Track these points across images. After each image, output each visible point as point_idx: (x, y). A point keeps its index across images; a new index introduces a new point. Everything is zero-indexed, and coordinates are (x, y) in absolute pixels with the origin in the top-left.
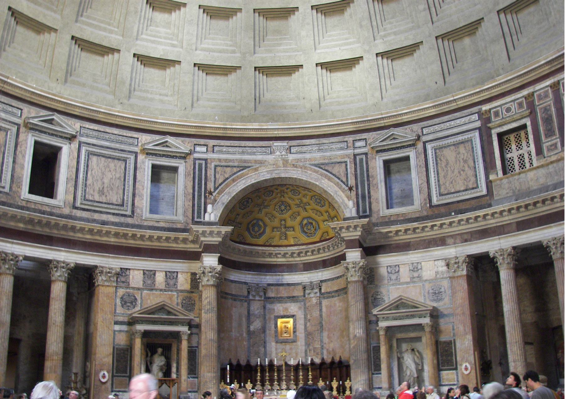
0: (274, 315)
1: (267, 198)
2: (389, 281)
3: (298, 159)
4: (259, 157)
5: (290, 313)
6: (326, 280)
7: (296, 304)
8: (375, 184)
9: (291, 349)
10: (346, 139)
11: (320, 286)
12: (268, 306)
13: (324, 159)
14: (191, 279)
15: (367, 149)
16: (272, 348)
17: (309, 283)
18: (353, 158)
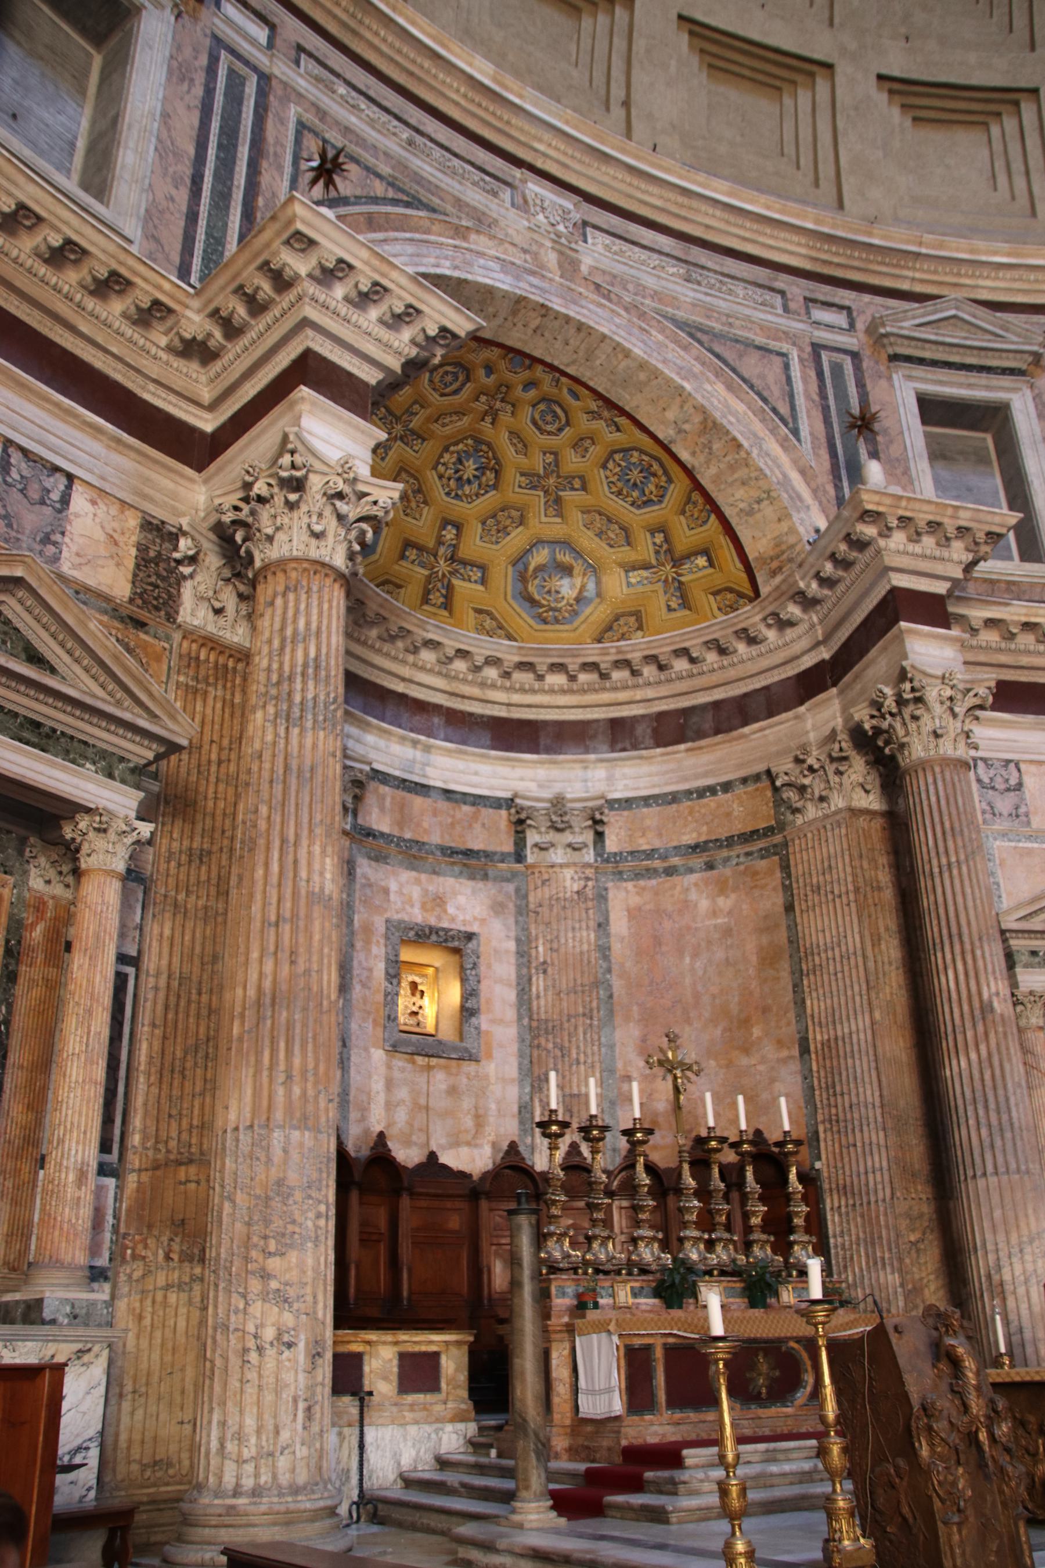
0: (387, 915)
1: (434, 398)
2: (988, 816)
3: (615, 277)
4: (475, 197)
5: (453, 919)
6: (628, 801)
7: (480, 885)
8: (897, 460)
9: (453, 1091)
10: (779, 285)
11: (601, 822)
12: (365, 867)
13: (708, 317)
14: (142, 549)
15: (855, 341)
16: (370, 1077)
17: (547, 805)
18: (809, 349)
